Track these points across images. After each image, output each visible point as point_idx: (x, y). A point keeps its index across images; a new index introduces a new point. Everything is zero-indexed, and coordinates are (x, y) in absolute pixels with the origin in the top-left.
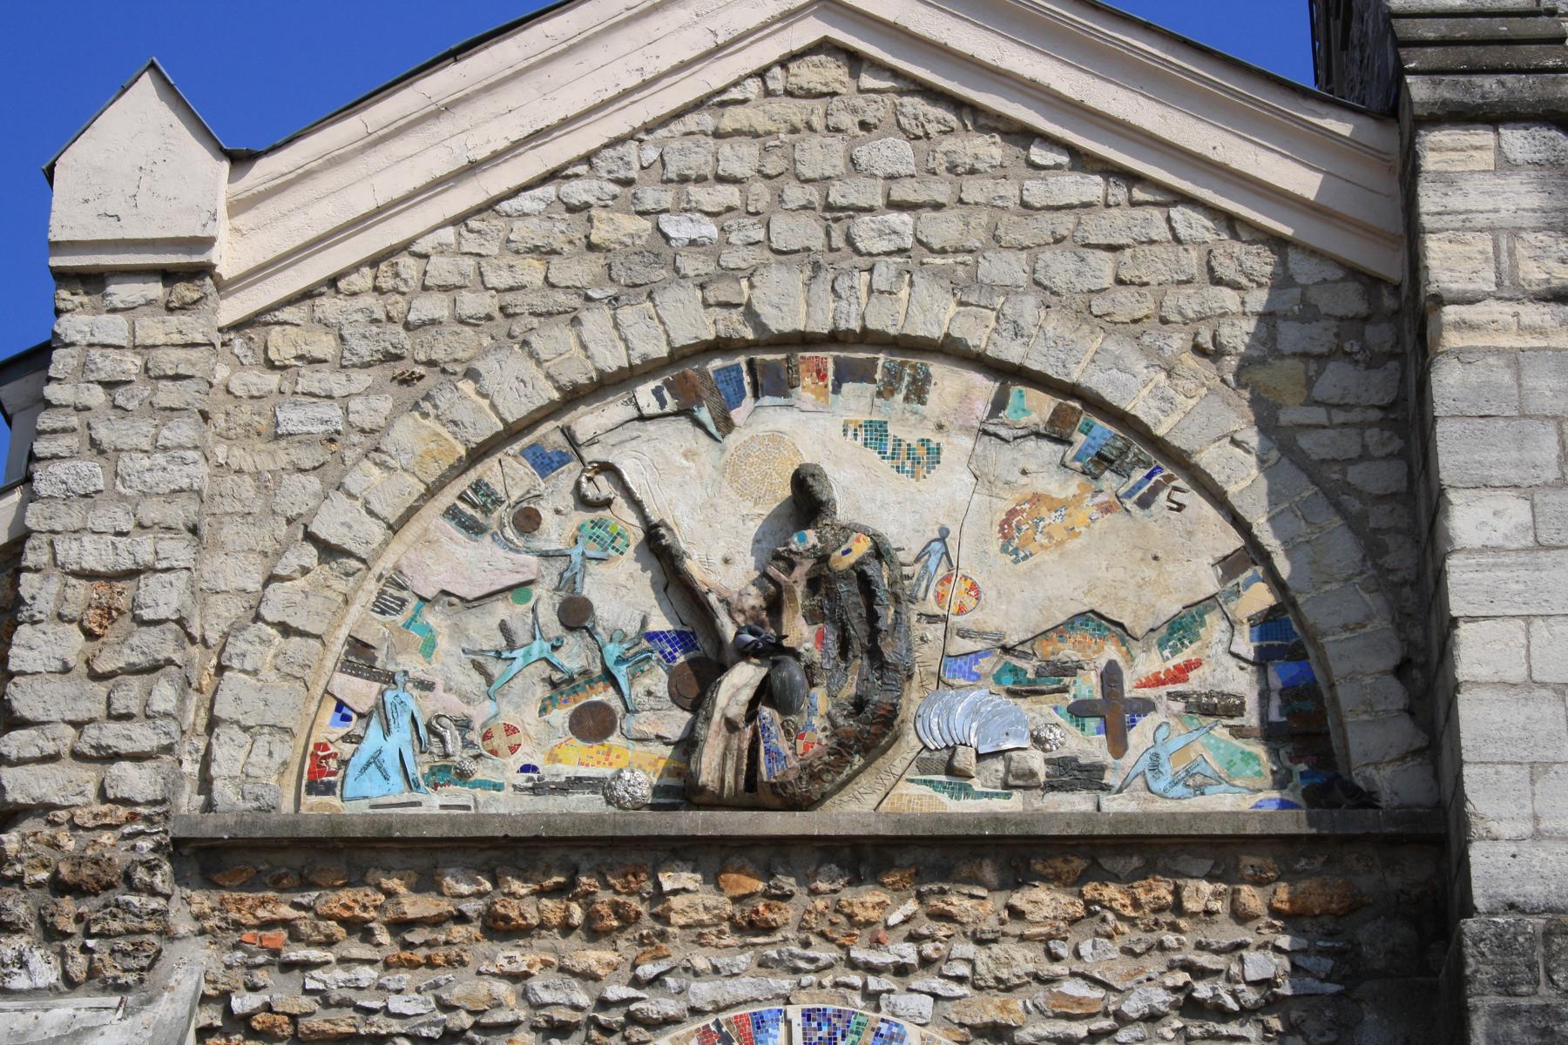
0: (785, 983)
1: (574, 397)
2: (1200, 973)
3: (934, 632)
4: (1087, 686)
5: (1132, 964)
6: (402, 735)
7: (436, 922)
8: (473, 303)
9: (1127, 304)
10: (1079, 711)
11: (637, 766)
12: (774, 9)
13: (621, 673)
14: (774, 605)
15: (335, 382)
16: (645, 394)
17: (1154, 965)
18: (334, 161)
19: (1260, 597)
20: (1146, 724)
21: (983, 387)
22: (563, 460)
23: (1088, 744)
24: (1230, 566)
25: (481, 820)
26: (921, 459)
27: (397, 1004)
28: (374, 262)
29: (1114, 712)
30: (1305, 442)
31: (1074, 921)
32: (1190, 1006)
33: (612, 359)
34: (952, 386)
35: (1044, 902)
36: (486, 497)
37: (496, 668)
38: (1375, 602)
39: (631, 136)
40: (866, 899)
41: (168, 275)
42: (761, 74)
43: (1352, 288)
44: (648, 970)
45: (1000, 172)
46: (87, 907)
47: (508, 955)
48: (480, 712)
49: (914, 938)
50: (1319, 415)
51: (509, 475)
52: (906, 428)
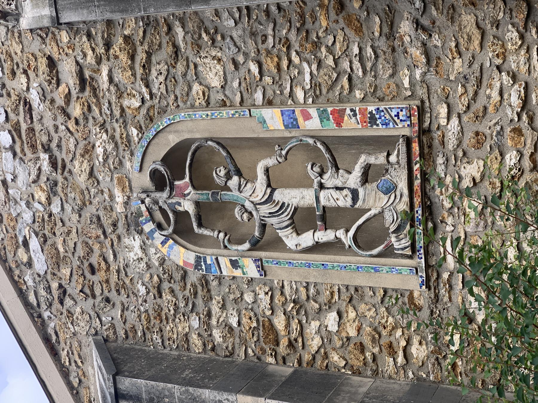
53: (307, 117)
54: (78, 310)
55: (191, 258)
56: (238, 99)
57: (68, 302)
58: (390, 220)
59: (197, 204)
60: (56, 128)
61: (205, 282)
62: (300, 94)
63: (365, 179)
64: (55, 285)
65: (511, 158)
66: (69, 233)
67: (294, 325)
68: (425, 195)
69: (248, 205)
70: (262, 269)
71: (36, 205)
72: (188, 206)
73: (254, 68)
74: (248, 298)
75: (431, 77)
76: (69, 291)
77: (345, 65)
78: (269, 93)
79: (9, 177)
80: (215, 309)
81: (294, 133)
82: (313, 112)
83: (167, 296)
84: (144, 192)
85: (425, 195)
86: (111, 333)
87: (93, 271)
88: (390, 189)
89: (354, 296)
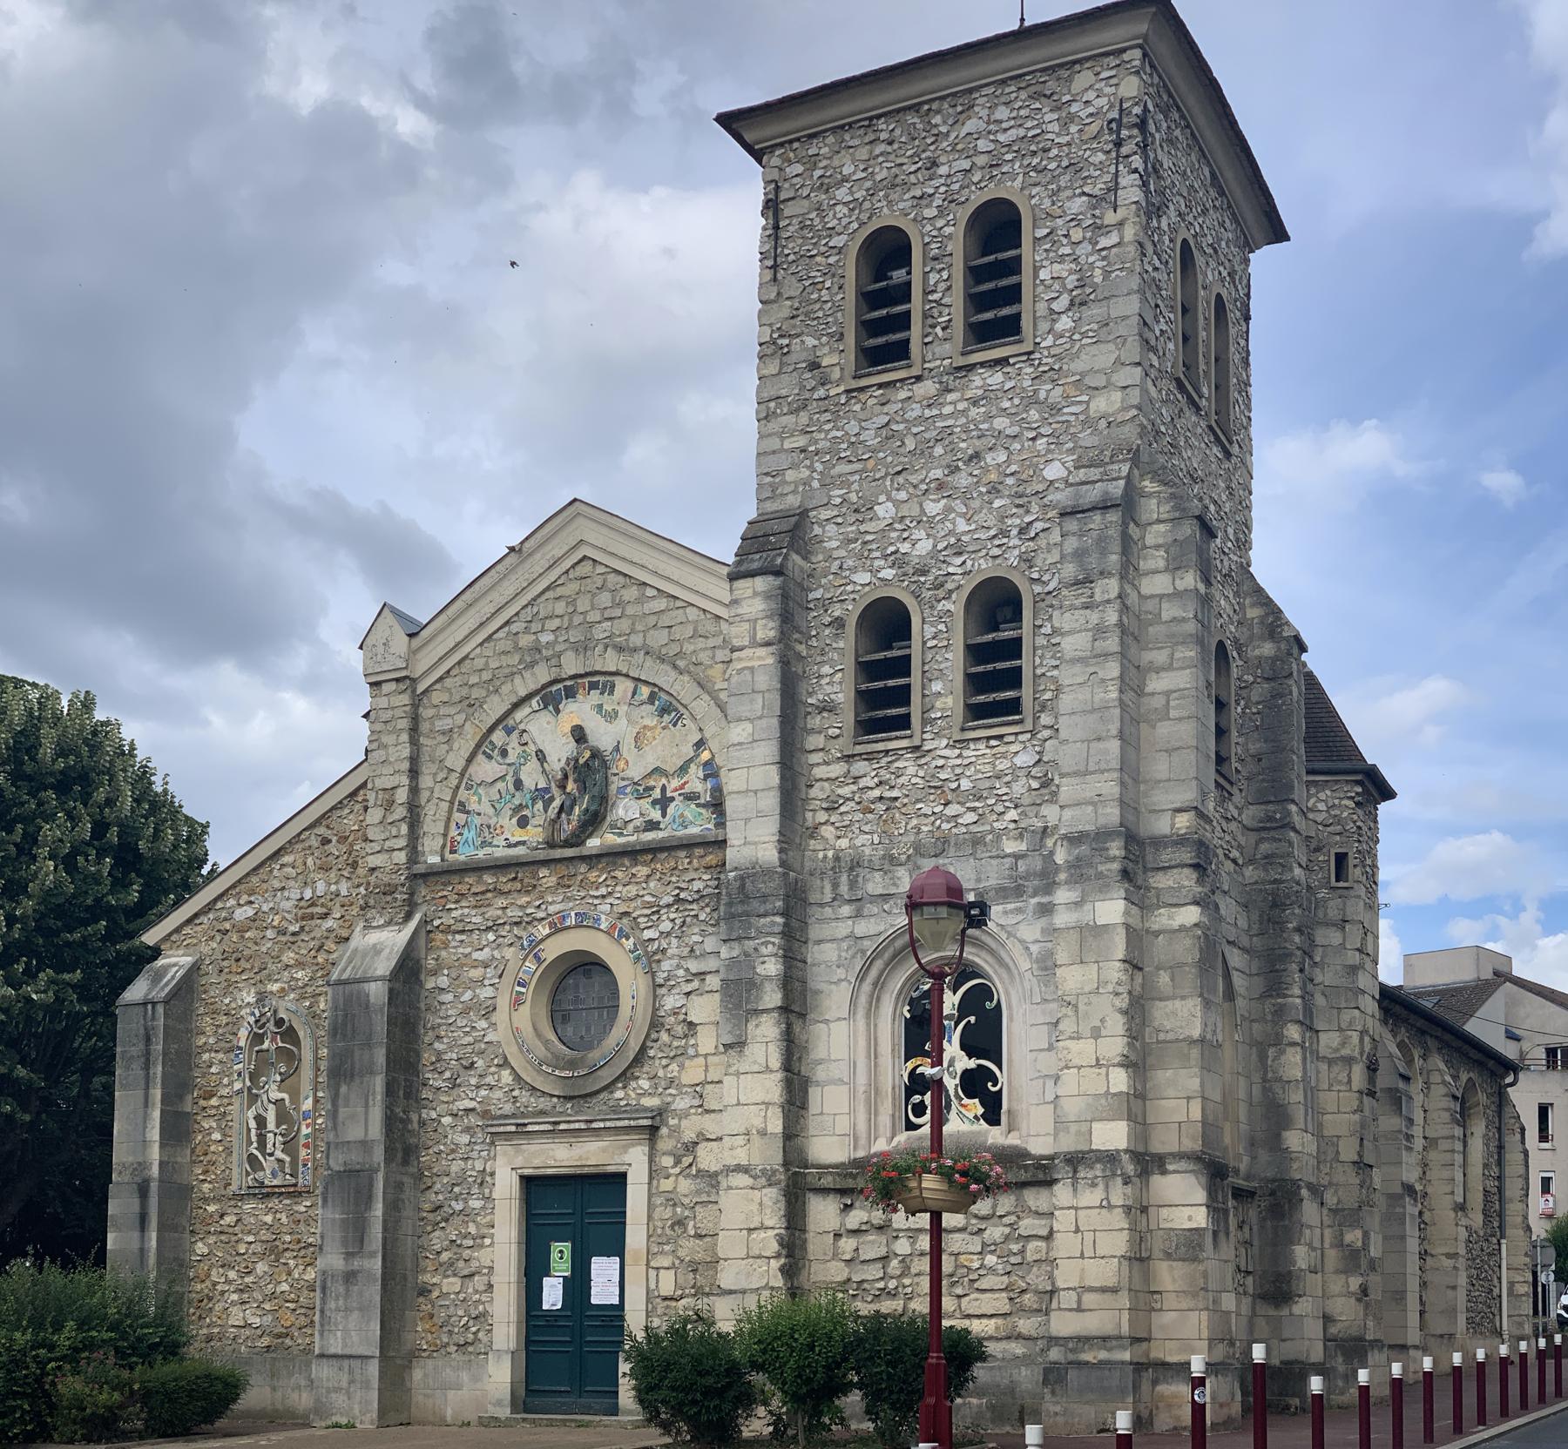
1: (516, 706)
2: (682, 889)
4: (657, 794)
7: (483, 893)
8: (486, 676)
9: (675, 648)
10: (654, 803)
11: (534, 834)
12: (566, 548)
14: (566, 777)
15: (452, 710)
18: (442, 630)
19: (706, 756)
20: (673, 805)
21: (630, 685)
22: (514, 729)
23: (656, 815)
24: (700, 744)
26: (612, 716)
28: (459, 663)
29: (664, 803)
31: (648, 876)
32: (678, 900)
33: (523, 693)
35: (642, 871)
41: (397, 680)
42: (567, 572)
46: (389, 898)
48: (492, 822)
51: (498, 737)
55: (242, 1044)
61: (231, 1050)
63: (279, 1160)
64: (227, 926)
65: (288, 1238)
67: (213, 1112)
70: (239, 1092)
72: (266, 1046)
80: (220, 1056)
83: (224, 1020)
88: (274, 1174)
89: (228, 1151)
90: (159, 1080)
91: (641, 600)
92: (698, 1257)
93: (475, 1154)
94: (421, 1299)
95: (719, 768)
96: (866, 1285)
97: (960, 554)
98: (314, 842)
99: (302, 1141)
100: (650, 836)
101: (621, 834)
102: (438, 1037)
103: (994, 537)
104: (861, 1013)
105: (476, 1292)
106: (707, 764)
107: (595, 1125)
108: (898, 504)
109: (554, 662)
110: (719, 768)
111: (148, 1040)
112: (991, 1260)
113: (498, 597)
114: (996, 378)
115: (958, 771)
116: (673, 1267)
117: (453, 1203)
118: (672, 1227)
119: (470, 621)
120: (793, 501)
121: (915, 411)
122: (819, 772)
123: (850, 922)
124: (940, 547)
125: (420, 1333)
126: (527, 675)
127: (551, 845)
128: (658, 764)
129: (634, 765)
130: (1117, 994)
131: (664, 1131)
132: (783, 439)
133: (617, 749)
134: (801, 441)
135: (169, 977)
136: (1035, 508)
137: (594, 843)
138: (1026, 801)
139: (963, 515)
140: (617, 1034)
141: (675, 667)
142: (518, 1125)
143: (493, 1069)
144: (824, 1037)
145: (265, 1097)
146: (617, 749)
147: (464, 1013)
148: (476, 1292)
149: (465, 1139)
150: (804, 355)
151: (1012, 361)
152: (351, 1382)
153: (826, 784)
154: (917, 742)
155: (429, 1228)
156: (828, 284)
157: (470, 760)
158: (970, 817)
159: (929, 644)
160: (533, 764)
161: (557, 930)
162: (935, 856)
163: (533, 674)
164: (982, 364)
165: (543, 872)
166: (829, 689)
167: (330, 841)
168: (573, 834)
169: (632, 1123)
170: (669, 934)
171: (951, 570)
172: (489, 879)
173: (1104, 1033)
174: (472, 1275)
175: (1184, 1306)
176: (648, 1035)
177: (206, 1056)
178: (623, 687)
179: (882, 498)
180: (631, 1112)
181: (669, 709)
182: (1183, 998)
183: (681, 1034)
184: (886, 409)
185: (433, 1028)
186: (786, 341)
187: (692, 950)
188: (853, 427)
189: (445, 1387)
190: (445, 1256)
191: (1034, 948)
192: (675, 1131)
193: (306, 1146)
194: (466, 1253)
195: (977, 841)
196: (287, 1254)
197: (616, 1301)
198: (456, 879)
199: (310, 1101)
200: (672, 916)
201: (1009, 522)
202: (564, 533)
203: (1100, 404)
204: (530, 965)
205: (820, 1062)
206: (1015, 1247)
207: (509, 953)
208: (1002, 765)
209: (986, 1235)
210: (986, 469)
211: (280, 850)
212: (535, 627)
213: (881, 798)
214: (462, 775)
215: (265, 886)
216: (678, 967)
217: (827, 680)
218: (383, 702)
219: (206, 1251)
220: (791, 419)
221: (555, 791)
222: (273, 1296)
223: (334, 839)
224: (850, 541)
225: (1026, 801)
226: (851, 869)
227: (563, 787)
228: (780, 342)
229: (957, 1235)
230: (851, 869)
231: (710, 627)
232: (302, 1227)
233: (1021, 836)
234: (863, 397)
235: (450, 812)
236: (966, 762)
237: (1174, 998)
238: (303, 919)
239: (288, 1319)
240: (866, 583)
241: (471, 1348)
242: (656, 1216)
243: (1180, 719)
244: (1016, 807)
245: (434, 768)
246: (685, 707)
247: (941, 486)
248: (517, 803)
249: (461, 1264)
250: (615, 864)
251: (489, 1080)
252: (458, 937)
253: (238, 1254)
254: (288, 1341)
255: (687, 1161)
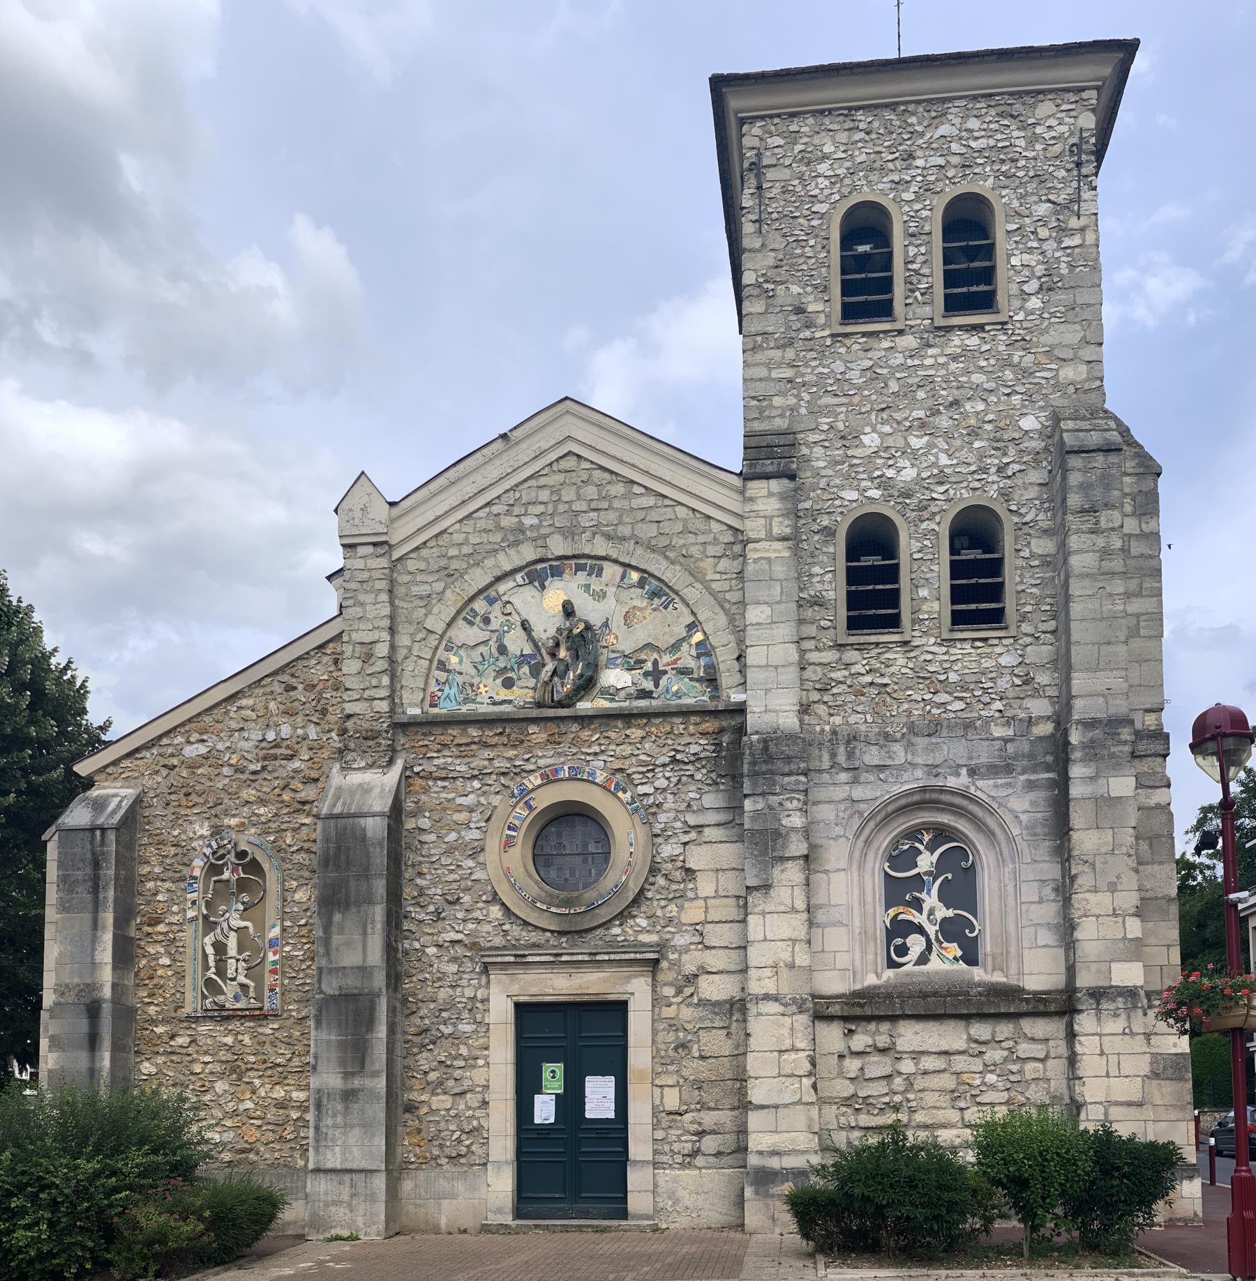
0: (562, 759)
1: (498, 579)
2: (677, 751)
3: (605, 651)
5: (659, 749)
6: (454, 690)
7: (467, 744)
9: (663, 542)
10: (646, 674)
11: (522, 694)
12: (553, 442)
13: (515, 667)
15: (430, 578)
16: (519, 577)
17: (665, 750)
19: (698, 637)
20: (666, 676)
21: (619, 570)
23: (648, 685)
24: (691, 627)
25: (475, 715)
26: (601, 596)
27: (458, 768)
28: (437, 536)
30: (714, 585)
31: (643, 738)
33: (507, 567)
34: (611, 571)
35: (635, 733)
36: (475, 614)
37: (480, 667)
38: (732, 637)
39: (511, 489)
40: (585, 734)
42: (550, 465)
43: (730, 532)
44: (527, 756)
45: (624, 497)
47: (487, 753)
48: (476, 681)
49: (600, 745)
50: (718, 577)
51: (480, 606)
52: (596, 585)
53: (275, 954)
54: (160, 779)
55: (197, 873)
56: (288, 910)
57: (164, 772)
58: (220, 999)
59: (228, 881)
60: (277, 778)
61: (182, 879)
62: (287, 949)
63: (242, 986)
64: (175, 761)
65: (252, 1059)
66: (210, 780)
67: (161, 938)
68: (234, 1017)
69: (227, 915)
71: (228, 756)
72: (226, 875)
73: (303, 922)
74: (175, 908)
75: (292, 1020)
76: (173, 773)
77: (301, 975)
78: (289, 930)
79: (246, 735)
80: (168, 885)
81: (267, 945)
82: (277, 957)
83: (173, 851)
84: (236, 844)
85: (234, 1017)
86: (145, 804)
87: (187, 795)
88: (236, 998)
89: (180, 975)
90: (110, 904)
91: (628, 496)
92: (701, 1076)
93: (464, 983)
94: (407, 1116)
95: (714, 648)
96: (871, 1100)
97: (941, 483)
98: (278, 688)
99: (269, 967)
100: (643, 703)
101: (612, 700)
102: (420, 874)
103: (974, 472)
104: (855, 867)
105: (469, 1108)
106: (698, 644)
107: (599, 958)
108: (883, 436)
109: (540, 543)
110: (714, 648)
111: (96, 864)
112: (991, 1078)
113: (481, 480)
114: (973, 341)
115: (946, 665)
116: (678, 1085)
117: (442, 1027)
118: (676, 1049)
119: (451, 498)
120: (780, 424)
121: (898, 359)
122: (814, 657)
123: (847, 787)
124: (924, 475)
125: (408, 1147)
126: (512, 552)
127: (539, 705)
128: (650, 640)
129: (623, 640)
130: (1130, 856)
131: (664, 964)
132: (770, 369)
133: (606, 625)
134: (789, 373)
135: (110, 808)
136: (1012, 451)
137: (584, 706)
138: (1011, 694)
139: (946, 451)
140: (613, 877)
141: (666, 557)
142: (516, 956)
143: (481, 905)
144: (824, 885)
145: (225, 925)
146: (606, 625)
147: (449, 851)
148: (469, 1108)
149: (453, 968)
150: (790, 300)
151: (987, 328)
152: (353, 1196)
153: (818, 669)
154: (907, 638)
155: (415, 1050)
156: (812, 242)
157: (449, 625)
158: (959, 705)
159: (916, 556)
160: (518, 633)
161: (550, 779)
162: (929, 735)
163: (518, 552)
164: (960, 327)
165: (532, 729)
166: (819, 587)
167: (295, 688)
168: (568, 697)
169: (638, 956)
170: (664, 790)
171: (935, 496)
172: (474, 732)
173: (1119, 888)
174: (463, 1093)
175: (1173, 1117)
176: (647, 879)
177: (150, 885)
178: (611, 571)
179: (868, 429)
180: (629, 946)
181: (660, 592)
182: (1161, 863)
183: (679, 879)
184: (870, 354)
185: (413, 865)
186: (771, 286)
187: (689, 806)
188: (839, 366)
189: (439, 1197)
190: (433, 1076)
191: (1024, 817)
192: (675, 964)
193: (274, 972)
194: (457, 1073)
195: (968, 726)
196: (251, 1074)
197: (612, 1115)
198: (438, 730)
199: (276, 931)
200: (668, 774)
201: (989, 461)
202: (550, 429)
203: (1067, 373)
204: (521, 811)
205: (820, 907)
206: (1014, 1068)
207: (496, 800)
208: (987, 663)
209: (987, 1057)
210: (965, 415)
211: (237, 693)
212: (517, 510)
213: (872, 684)
214: (442, 636)
215: (220, 726)
216: (675, 819)
217: (818, 579)
218: (359, 564)
219: (153, 1070)
220: (777, 354)
221: (547, 658)
222: (235, 1113)
223: (300, 687)
224: (838, 463)
225: (1011, 694)
226: (849, 742)
227: (553, 655)
228: (766, 286)
229: (957, 1057)
230: (849, 742)
231: (699, 524)
232: (268, 1047)
233: (1008, 724)
234: (848, 342)
235: (430, 669)
236: (952, 658)
237: (1152, 863)
238: (265, 759)
239: (252, 1134)
240: (854, 499)
241: (465, 1158)
242: (660, 1038)
243: (1150, 637)
244: (1001, 699)
245: (412, 629)
246: (676, 593)
247: (923, 425)
248: (502, 665)
249: (451, 1083)
250: (608, 725)
251: (477, 914)
252: (439, 783)
253: (192, 1073)
254: (252, 1156)
255: (688, 991)
